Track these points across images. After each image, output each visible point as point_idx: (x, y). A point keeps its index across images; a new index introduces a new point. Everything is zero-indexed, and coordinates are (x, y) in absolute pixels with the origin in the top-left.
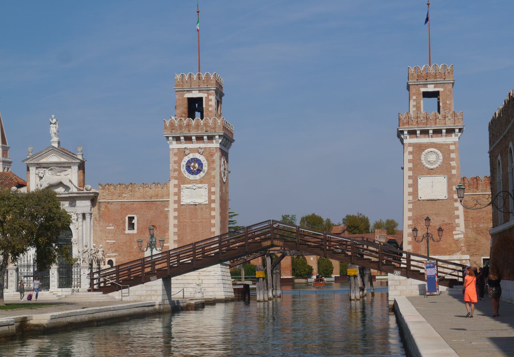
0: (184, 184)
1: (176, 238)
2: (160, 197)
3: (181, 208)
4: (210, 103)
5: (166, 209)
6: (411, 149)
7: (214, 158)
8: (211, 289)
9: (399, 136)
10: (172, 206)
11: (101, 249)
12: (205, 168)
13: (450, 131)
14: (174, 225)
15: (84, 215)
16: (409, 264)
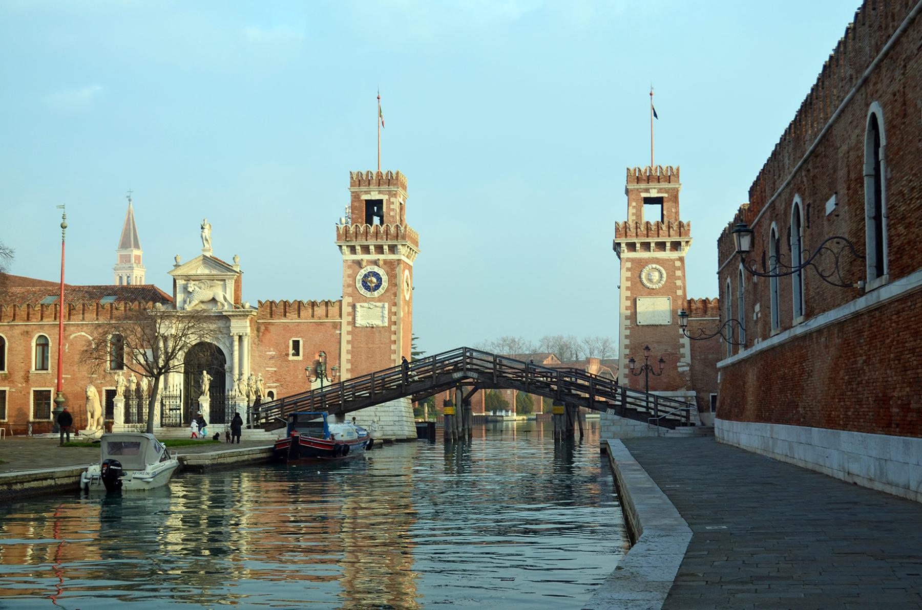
4: (392, 207)
6: (629, 265)
8: (390, 428)
9: (615, 249)
10: (346, 328)
12: (385, 284)
13: (676, 246)
16: (624, 401)
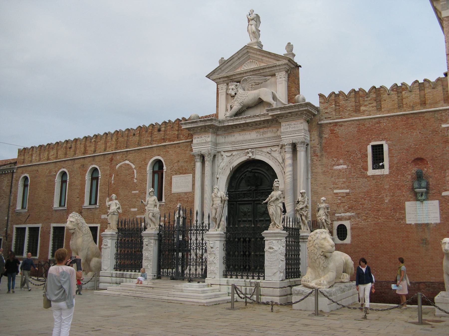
2: (431, 104)
11: (323, 205)
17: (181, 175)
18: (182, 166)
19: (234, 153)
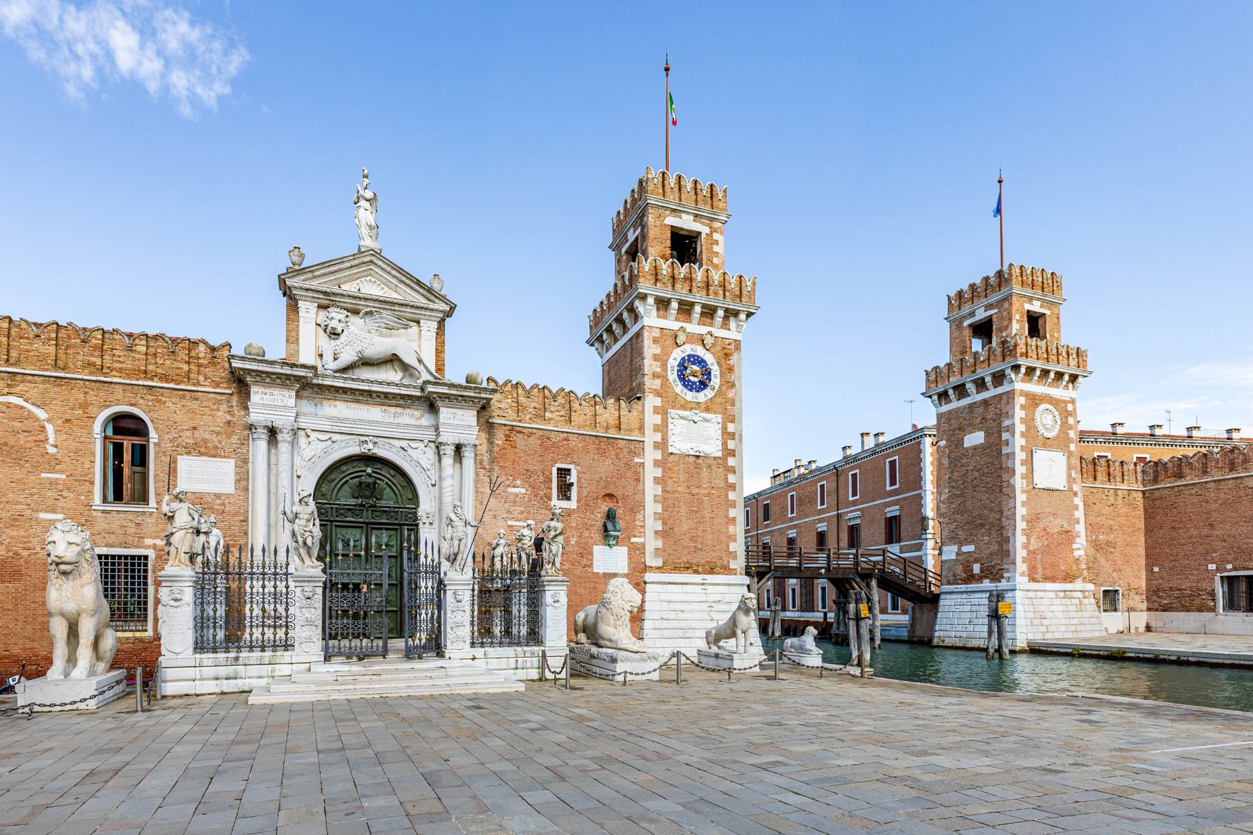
0: (673, 408)
1: (659, 526)
2: (626, 430)
3: (667, 460)
5: (637, 460)
7: (732, 362)
10: (651, 455)
12: (716, 381)
14: (655, 496)
15: (458, 448)
17: (203, 458)
18: (205, 441)
19: (336, 437)
